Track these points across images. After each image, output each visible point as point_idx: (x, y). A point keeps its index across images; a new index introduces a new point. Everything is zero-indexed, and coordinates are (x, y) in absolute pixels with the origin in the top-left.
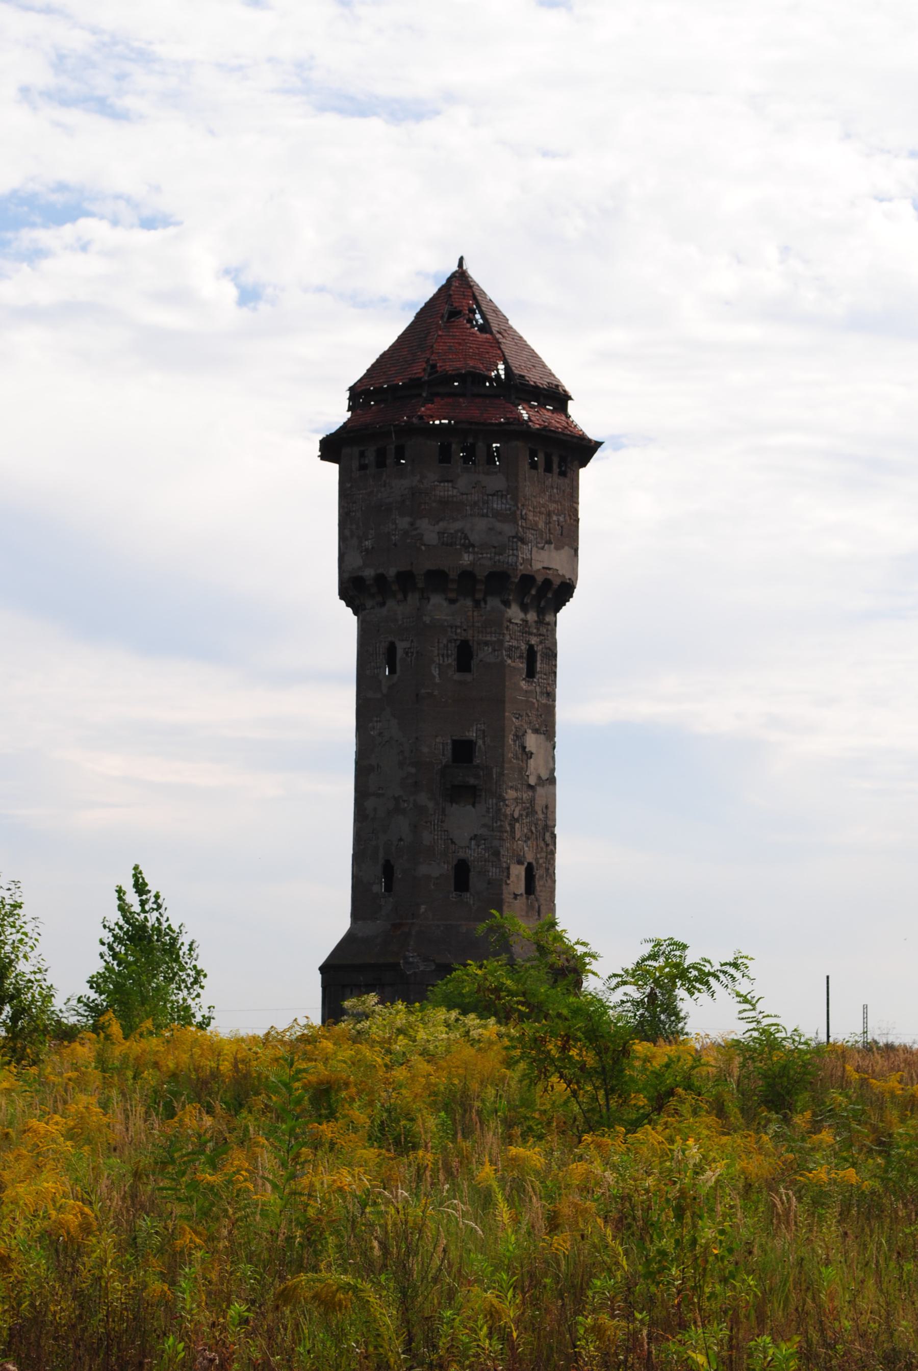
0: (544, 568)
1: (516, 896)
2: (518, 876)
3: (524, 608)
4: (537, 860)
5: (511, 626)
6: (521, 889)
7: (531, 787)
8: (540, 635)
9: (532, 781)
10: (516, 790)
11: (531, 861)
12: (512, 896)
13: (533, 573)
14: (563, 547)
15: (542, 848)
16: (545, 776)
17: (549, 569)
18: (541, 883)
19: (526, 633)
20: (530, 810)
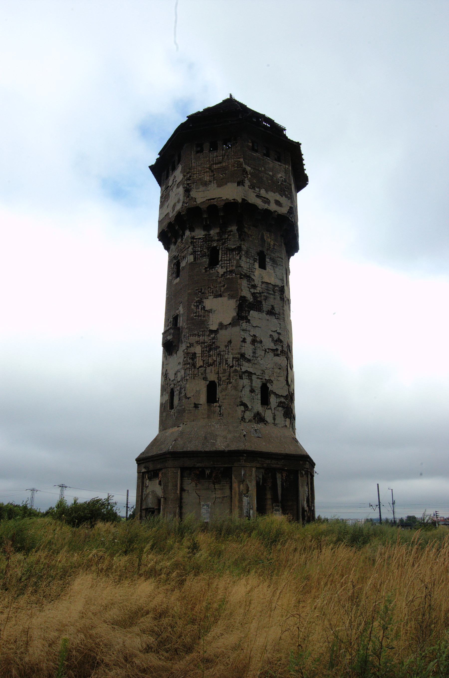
0: (209, 200)
1: (196, 406)
2: (198, 392)
3: (207, 228)
4: (219, 379)
5: (195, 240)
6: (203, 399)
7: (212, 332)
8: (223, 239)
9: (214, 327)
10: (199, 336)
11: (212, 379)
12: (193, 405)
13: (197, 205)
14: (226, 184)
15: (224, 370)
16: (227, 321)
17: (213, 199)
18: (224, 393)
19: (209, 241)
20: (211, 347)
